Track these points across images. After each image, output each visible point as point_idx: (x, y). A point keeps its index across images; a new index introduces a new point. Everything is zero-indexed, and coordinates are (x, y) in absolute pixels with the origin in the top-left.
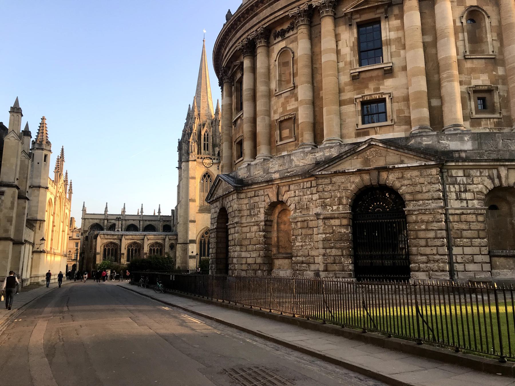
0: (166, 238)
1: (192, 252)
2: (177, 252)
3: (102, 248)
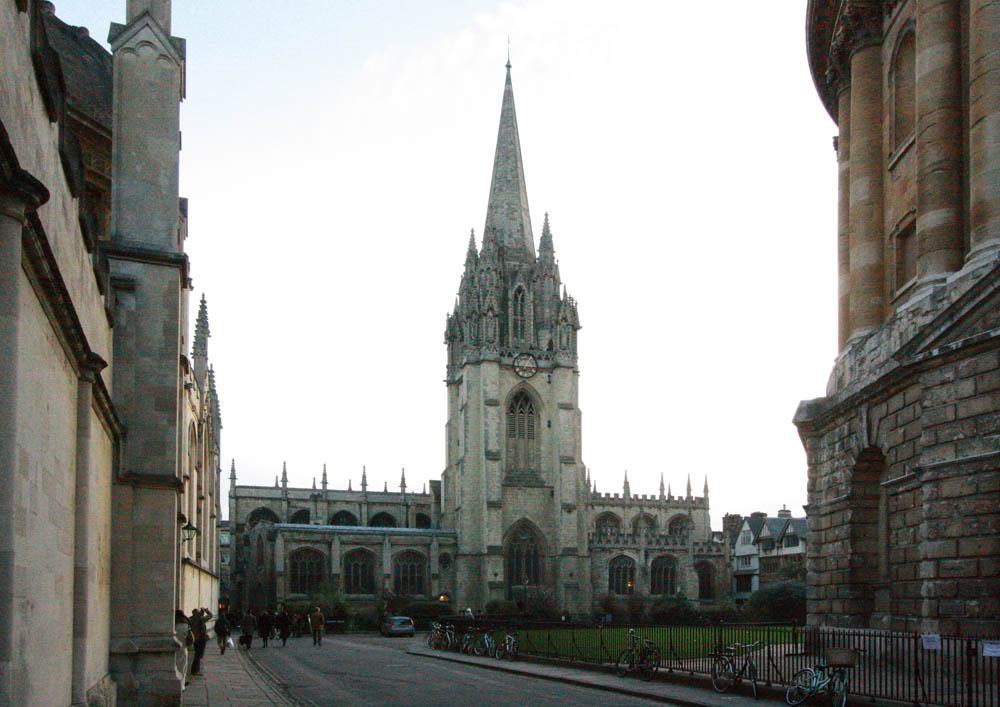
0: (432, 541)
1: (496, 575)
2: (458, 574)
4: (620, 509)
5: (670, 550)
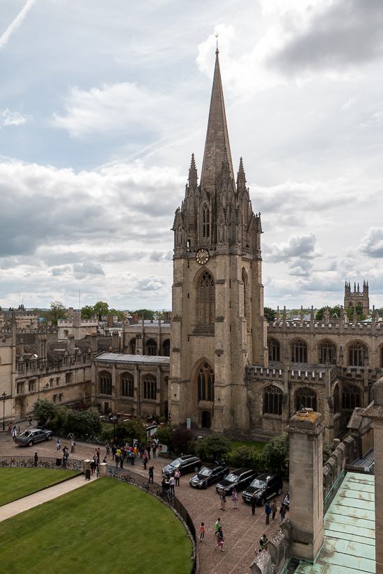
1: (175, 395)
3: (98, 377)
4: (336, 336)
5: (309, 384)
